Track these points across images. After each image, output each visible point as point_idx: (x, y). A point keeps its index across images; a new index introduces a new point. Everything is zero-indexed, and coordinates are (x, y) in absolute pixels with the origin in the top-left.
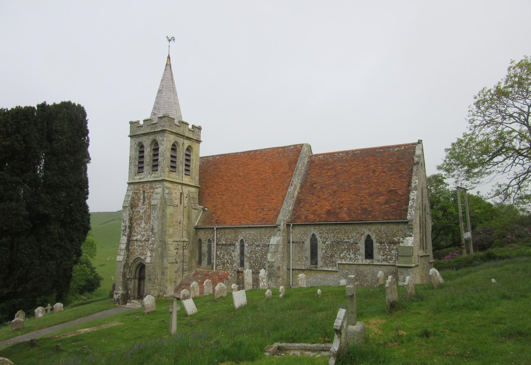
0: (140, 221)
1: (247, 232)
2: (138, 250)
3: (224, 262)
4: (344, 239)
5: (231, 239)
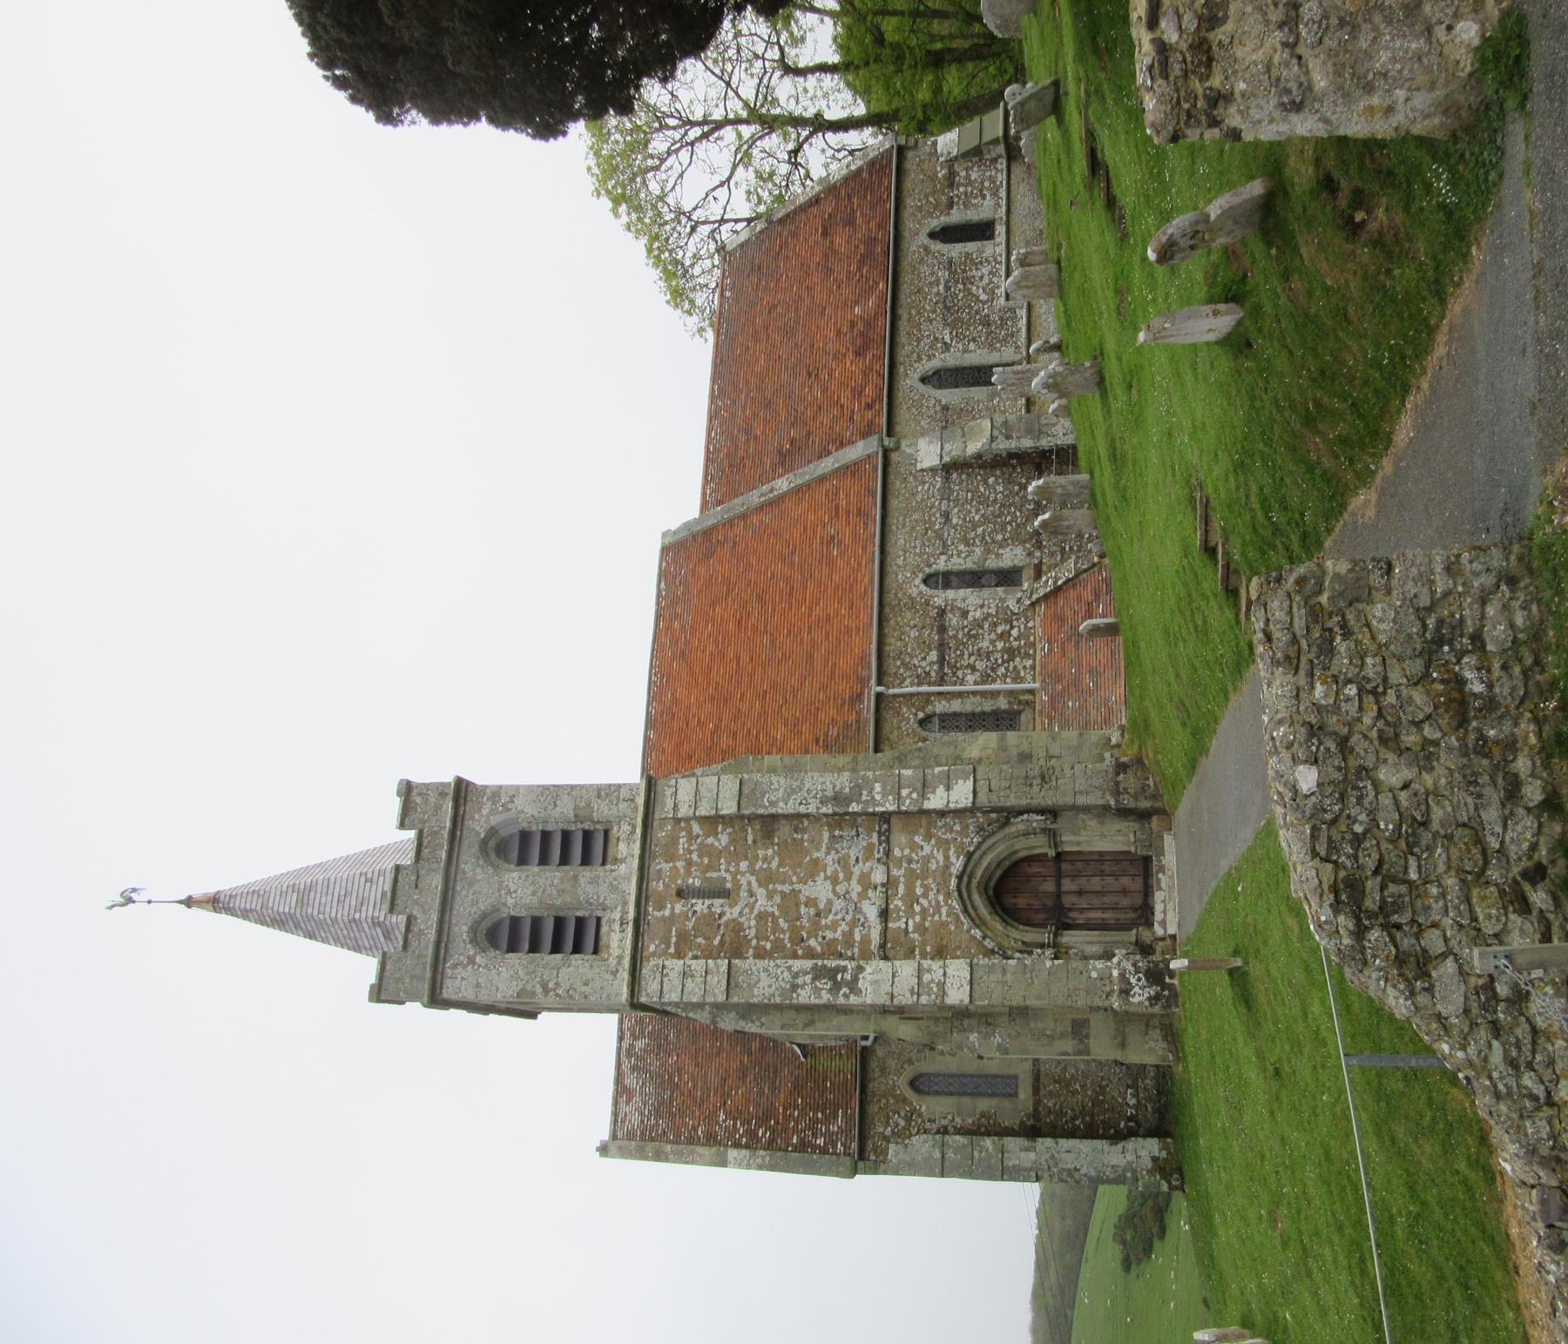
0: (803, 910)
1: (900, 561)
3: (1004, 650)
4: (938, 294)
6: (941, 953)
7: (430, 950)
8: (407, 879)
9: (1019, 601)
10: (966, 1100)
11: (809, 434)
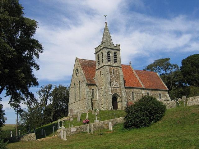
8: (112, 45)
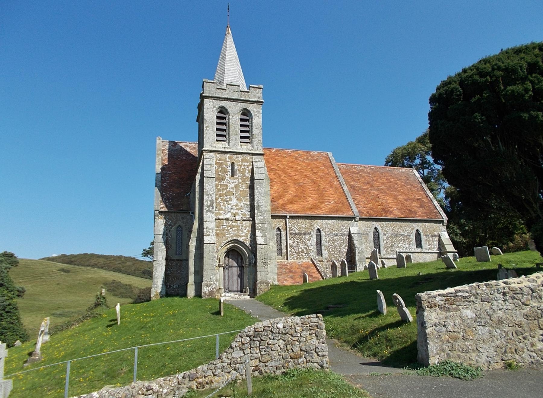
2: (231, 230)
3: (299, 251)
4: (400, 232)
5: (306, 228)
6: (217, 235)
7: (217, 96)
9: (312, 255)
10: (175, 241)
11: (360, 195)
